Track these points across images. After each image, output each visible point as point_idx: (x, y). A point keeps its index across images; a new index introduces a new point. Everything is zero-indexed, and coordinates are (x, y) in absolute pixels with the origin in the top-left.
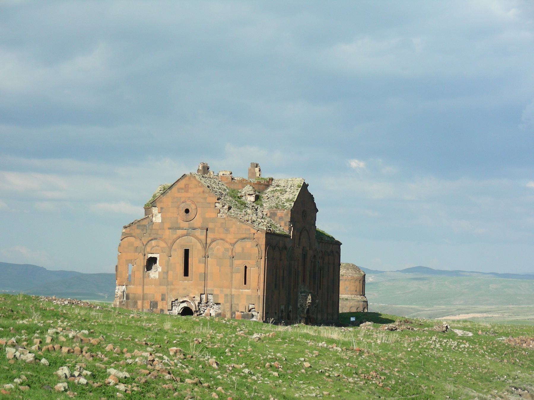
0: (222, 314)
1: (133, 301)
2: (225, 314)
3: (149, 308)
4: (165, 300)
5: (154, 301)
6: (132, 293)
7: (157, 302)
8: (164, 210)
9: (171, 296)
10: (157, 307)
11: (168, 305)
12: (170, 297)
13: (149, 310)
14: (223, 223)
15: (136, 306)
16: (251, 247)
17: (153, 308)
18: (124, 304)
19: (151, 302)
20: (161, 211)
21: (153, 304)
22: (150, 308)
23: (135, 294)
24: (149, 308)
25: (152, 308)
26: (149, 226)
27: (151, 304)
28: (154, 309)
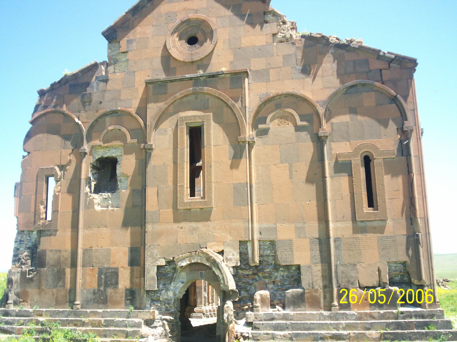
0: (307, 295)
1: (55, 269)
2: (316, 294)
3: (95, 286)
4: (140, 266)
5: (108, 269)
6: (51, 251)
7: (117, 269)
8: (135, 44)
9: (156, 251)
10: (117, 283)
11: (147, 276)
12: (152, 256)
13: (94, 293)
14: (291, 55)
15: (60, 283)
16: (377, 105)
17: (106, 286)
18: (31, 279)
19: (100, 272)
20: (128, 47)
21: (106, 277)
22: (99, 285)
23: (60, 251)
24: (96, 287)
25: (102, 288)
26: (98, 85)
27: (100, 278)
28: (110, 291)
